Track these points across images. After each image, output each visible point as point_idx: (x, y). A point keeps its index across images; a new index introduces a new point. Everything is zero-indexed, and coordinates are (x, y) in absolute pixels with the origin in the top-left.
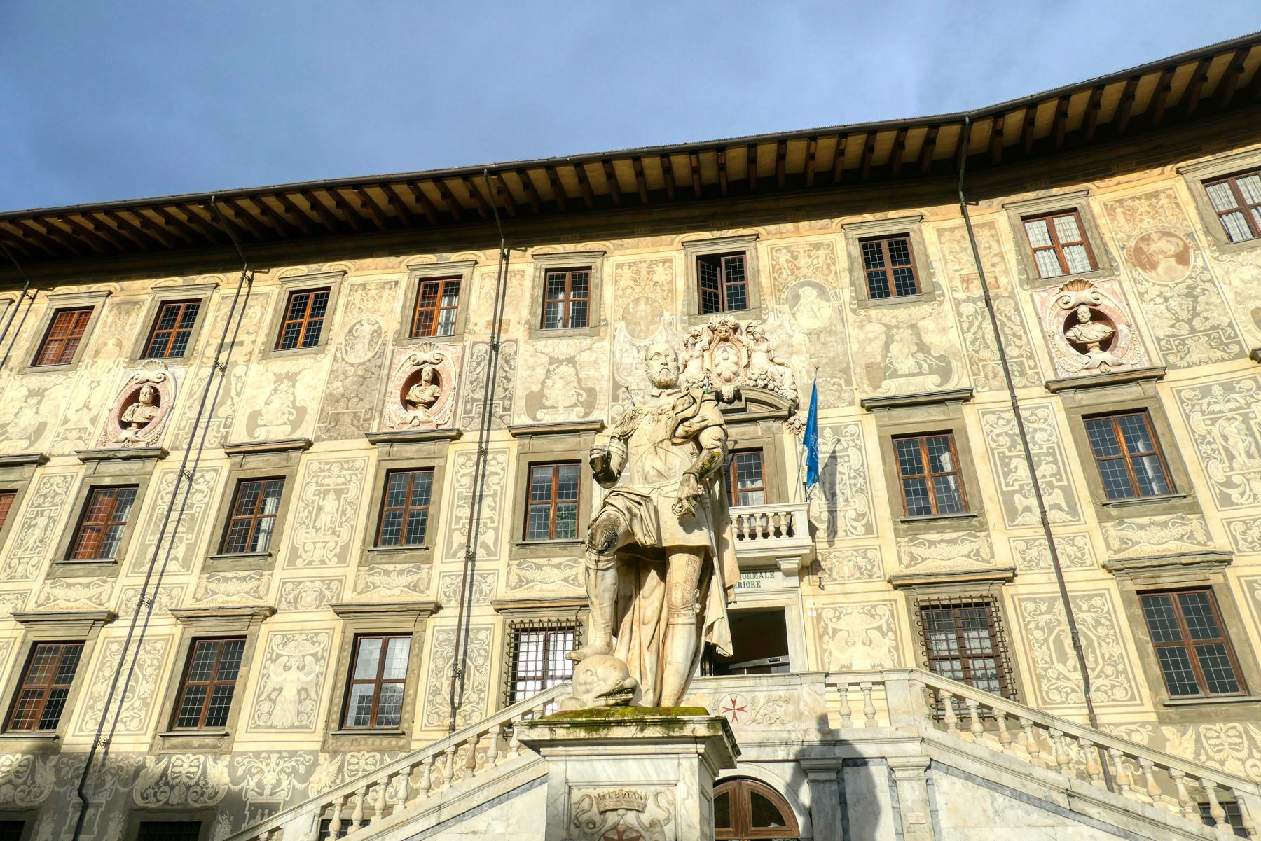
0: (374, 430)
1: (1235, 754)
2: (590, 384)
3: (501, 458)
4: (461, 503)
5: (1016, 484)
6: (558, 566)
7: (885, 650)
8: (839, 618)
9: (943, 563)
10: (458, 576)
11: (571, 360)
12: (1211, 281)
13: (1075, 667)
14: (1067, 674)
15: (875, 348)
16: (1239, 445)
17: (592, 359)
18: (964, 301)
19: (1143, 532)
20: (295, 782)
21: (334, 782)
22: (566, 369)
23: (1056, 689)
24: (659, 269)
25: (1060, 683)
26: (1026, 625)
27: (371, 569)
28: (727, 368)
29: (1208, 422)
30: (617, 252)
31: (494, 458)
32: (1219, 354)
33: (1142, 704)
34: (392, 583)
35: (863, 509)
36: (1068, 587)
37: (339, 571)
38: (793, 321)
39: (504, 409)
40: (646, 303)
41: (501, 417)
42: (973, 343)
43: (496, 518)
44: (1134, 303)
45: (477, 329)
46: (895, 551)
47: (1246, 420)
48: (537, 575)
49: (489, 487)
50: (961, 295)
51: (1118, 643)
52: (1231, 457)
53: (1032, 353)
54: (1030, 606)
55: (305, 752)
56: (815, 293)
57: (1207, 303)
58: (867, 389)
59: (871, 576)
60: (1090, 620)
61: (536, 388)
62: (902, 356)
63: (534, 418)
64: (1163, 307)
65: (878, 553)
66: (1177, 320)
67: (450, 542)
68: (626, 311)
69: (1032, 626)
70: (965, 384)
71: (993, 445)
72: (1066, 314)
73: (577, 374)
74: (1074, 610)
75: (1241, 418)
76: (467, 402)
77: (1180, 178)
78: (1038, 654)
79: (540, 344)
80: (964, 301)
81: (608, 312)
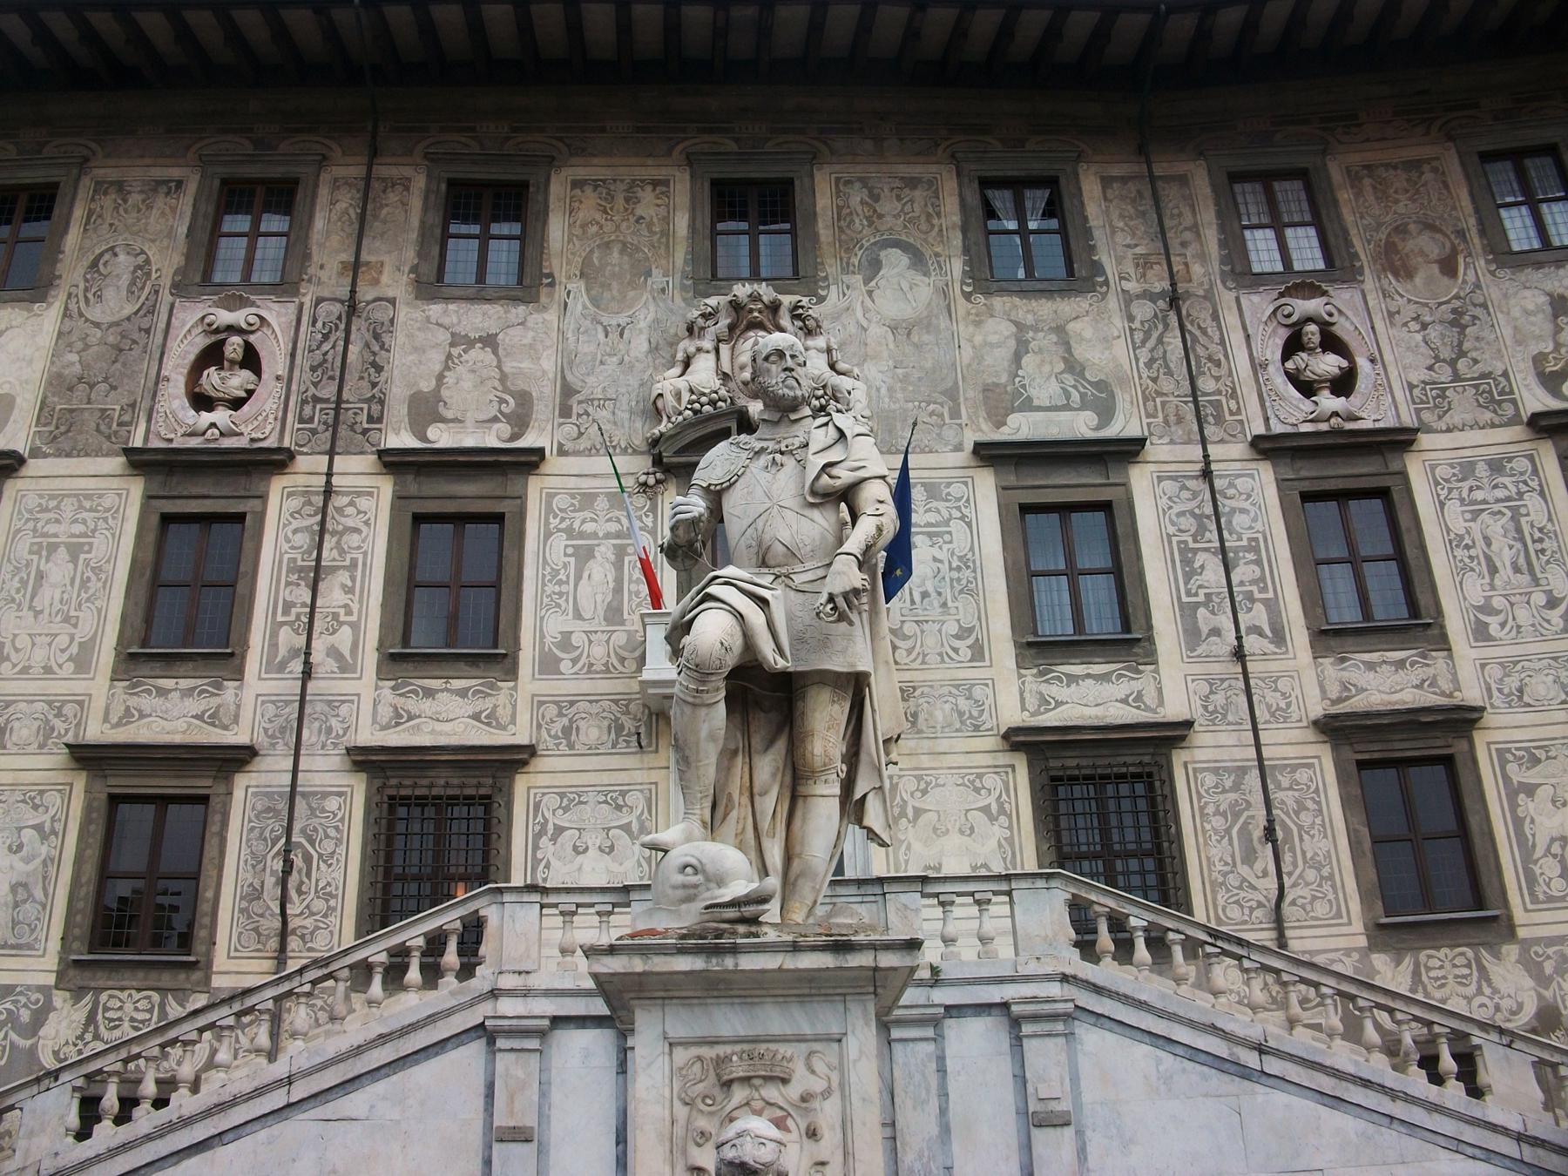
0: (138, 442)
1: (1461, 989)
2: (521, 385)
3: (363, 503)
5: (1202, 592)
6: (462, 693)
7: (993, 843)
8: (924, 792)
10: (287, 703)
11: (489, 341)
12: (1484, 306)
13: (1265, 874)
14: (1254, 881)
15: (999, 358)
16: (1505, 554)
17: (525, 341)
18: (1138, 297)
19: (1372, 674)
20: (13, 1036)
21: (81, 1037)
22: (479, 354)
23: (1237, 902)
24: (647, 195)
25: (1243, 894)
26: (1202, 809)
27: (135, 686)
29: (1468, 516)
30: (574, 160)
32: (1488, 415)
33: (1350, 923)
34: (172, 714)
36: (1266, 753)
37: (79, 687)
39: (370, 419)
40: (622, 252)
41: (365, 432)
42: (1149, 365)
43: (355, 607)
44: (1379, 325)
45: (324, 275)
46: (1015, 690)
47: (1516, 518)
48: (427, 706)
50: (1132, 286)
51: (1325, 837)
52: (1493, 570)
53: (1234, 389)
54: (1210, 780)
55: (29, 988)
56: (905, 260)
57: (1477, 339)
58: (984, 427)
59: (977, 728)
60: (1291, 804)
61: (427, 386)
63: (424, 439)
64: (1419, 337)
65: (989, 691)
66: (1437, 359)
67: (274, 645)
68: (587, 262)
69: (1210, 809)
70: (1133, 430)
71: (1171, 530)
72: (1284, 334)
73: (499, 367)
74: (1271, 787)
75: (1509, 514)
76: (304, 402)
77: (1451, 144)
78: (1215, 853)
79: (435, 310)
80: (1138, 297)
81: (555, 262)
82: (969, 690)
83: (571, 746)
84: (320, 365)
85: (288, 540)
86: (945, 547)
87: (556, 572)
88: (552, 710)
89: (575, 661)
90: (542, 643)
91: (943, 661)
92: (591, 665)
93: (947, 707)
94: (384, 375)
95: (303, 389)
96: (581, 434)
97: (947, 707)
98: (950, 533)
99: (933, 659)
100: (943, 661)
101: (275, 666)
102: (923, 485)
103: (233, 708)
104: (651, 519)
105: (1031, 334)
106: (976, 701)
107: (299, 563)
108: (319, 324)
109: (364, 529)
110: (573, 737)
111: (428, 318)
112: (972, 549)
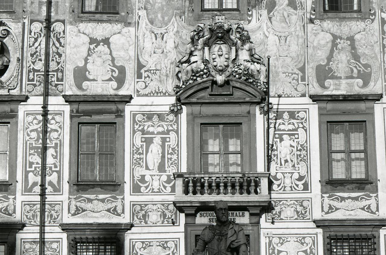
3: (58, 118)
4: (32, 152)
6: (103, 201)
8: (282, 244)
9: (348, 213)
28: (220, 62)
31: (53, 119)
35: (303, 172)
38: (269, 24)
39: (58, 80)
41: (56, 85)
43: (58, 164)
48: (89, 206)
49: (51, 140)
61: (81, 64)
62: (342, 62)
82: (302, 202)
83: (146, 223)
84: (35, 53)
85: (28, 135)
86: (296, 140)
87: (138, 149)
88: (138, 208)
89: (147, 187)
90: (133, 180)
91: (292, 190)
92: (153, 189)
93: (293, 209)
94: (63, 58)
95: (28, 66)
96: (146, 86)
97: (293, 209)
98: (298, 134)
99: (288, 189)
100: (292, 190)
101: (28, 190)
102: (288, 112)
103: (13, 207)
104: (176, 126)
105: (339, 40)
106: (304, 207)
107: (34, 145)
108: (33, 34)
109: (59, 129)
110: (147, 219)
111: (79, 30)
112: (306, 141)
